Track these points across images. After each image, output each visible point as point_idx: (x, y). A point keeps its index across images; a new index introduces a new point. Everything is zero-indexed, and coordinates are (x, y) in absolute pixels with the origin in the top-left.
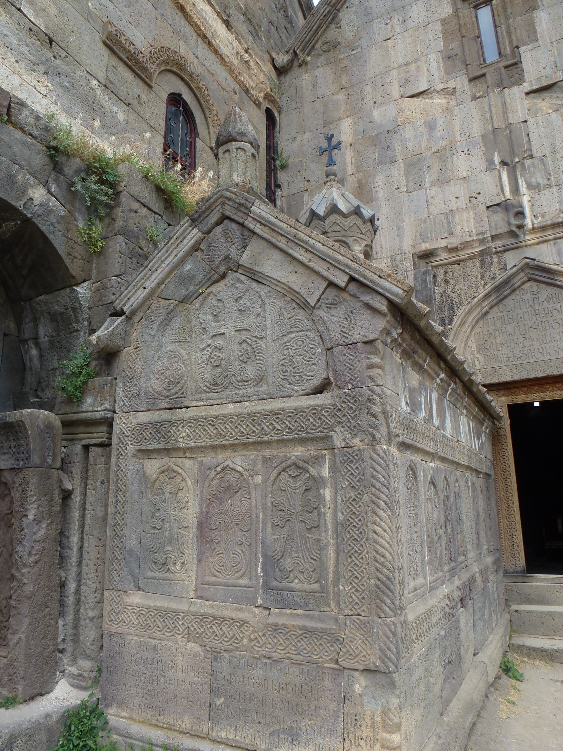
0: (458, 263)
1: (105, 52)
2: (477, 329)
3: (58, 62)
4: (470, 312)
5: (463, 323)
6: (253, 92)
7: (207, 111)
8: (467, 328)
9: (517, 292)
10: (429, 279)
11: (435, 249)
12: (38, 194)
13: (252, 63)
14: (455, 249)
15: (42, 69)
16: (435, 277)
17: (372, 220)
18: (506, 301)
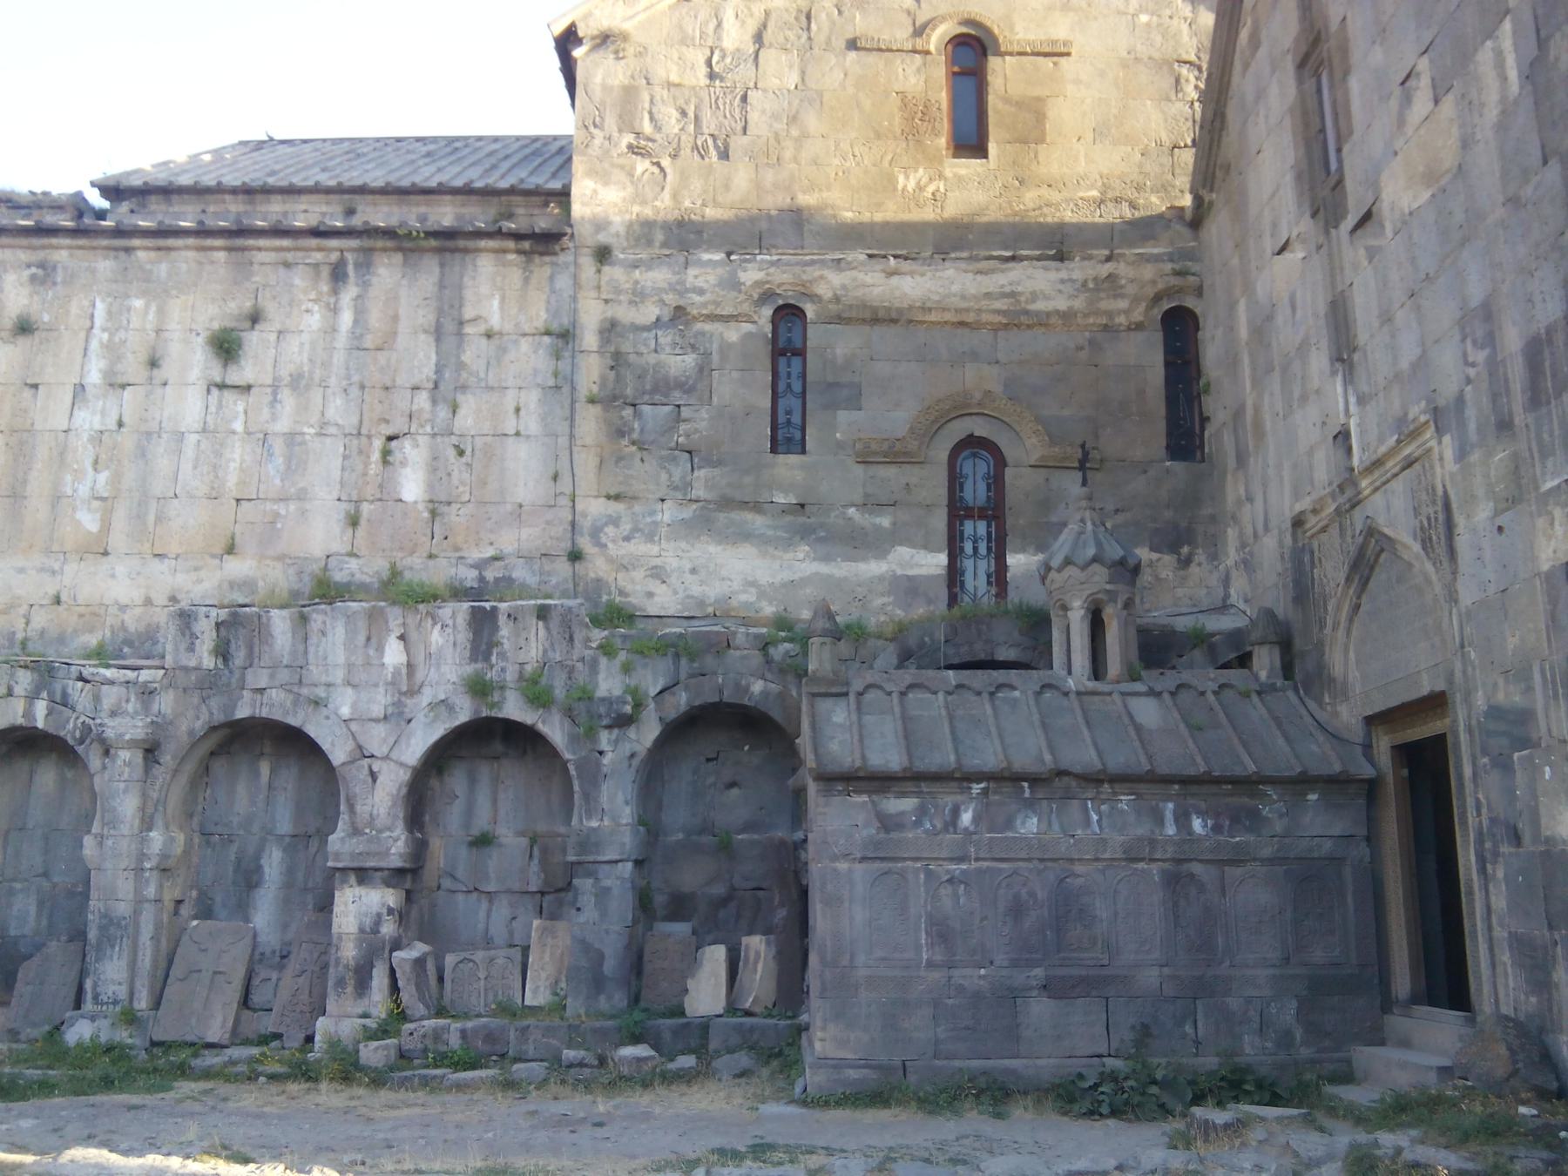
0: (1324, 530)
1: (859, 470)
2: (1354, 633)
3: (812, 520)
4: (1338, 608)
5: (1335, 628)
6: (1121, 319)
7: (1015, 426)
8: (1341, 633)
9: (1377, 570)
10: (1307, 558)
11: (1302, 513)
12: (757, 687)
13: (1122, 269)
14: (1315, 511)
15: (798, 538)
16: (1312, 553)
17: (1095, 560)
18: (1371, 584)
